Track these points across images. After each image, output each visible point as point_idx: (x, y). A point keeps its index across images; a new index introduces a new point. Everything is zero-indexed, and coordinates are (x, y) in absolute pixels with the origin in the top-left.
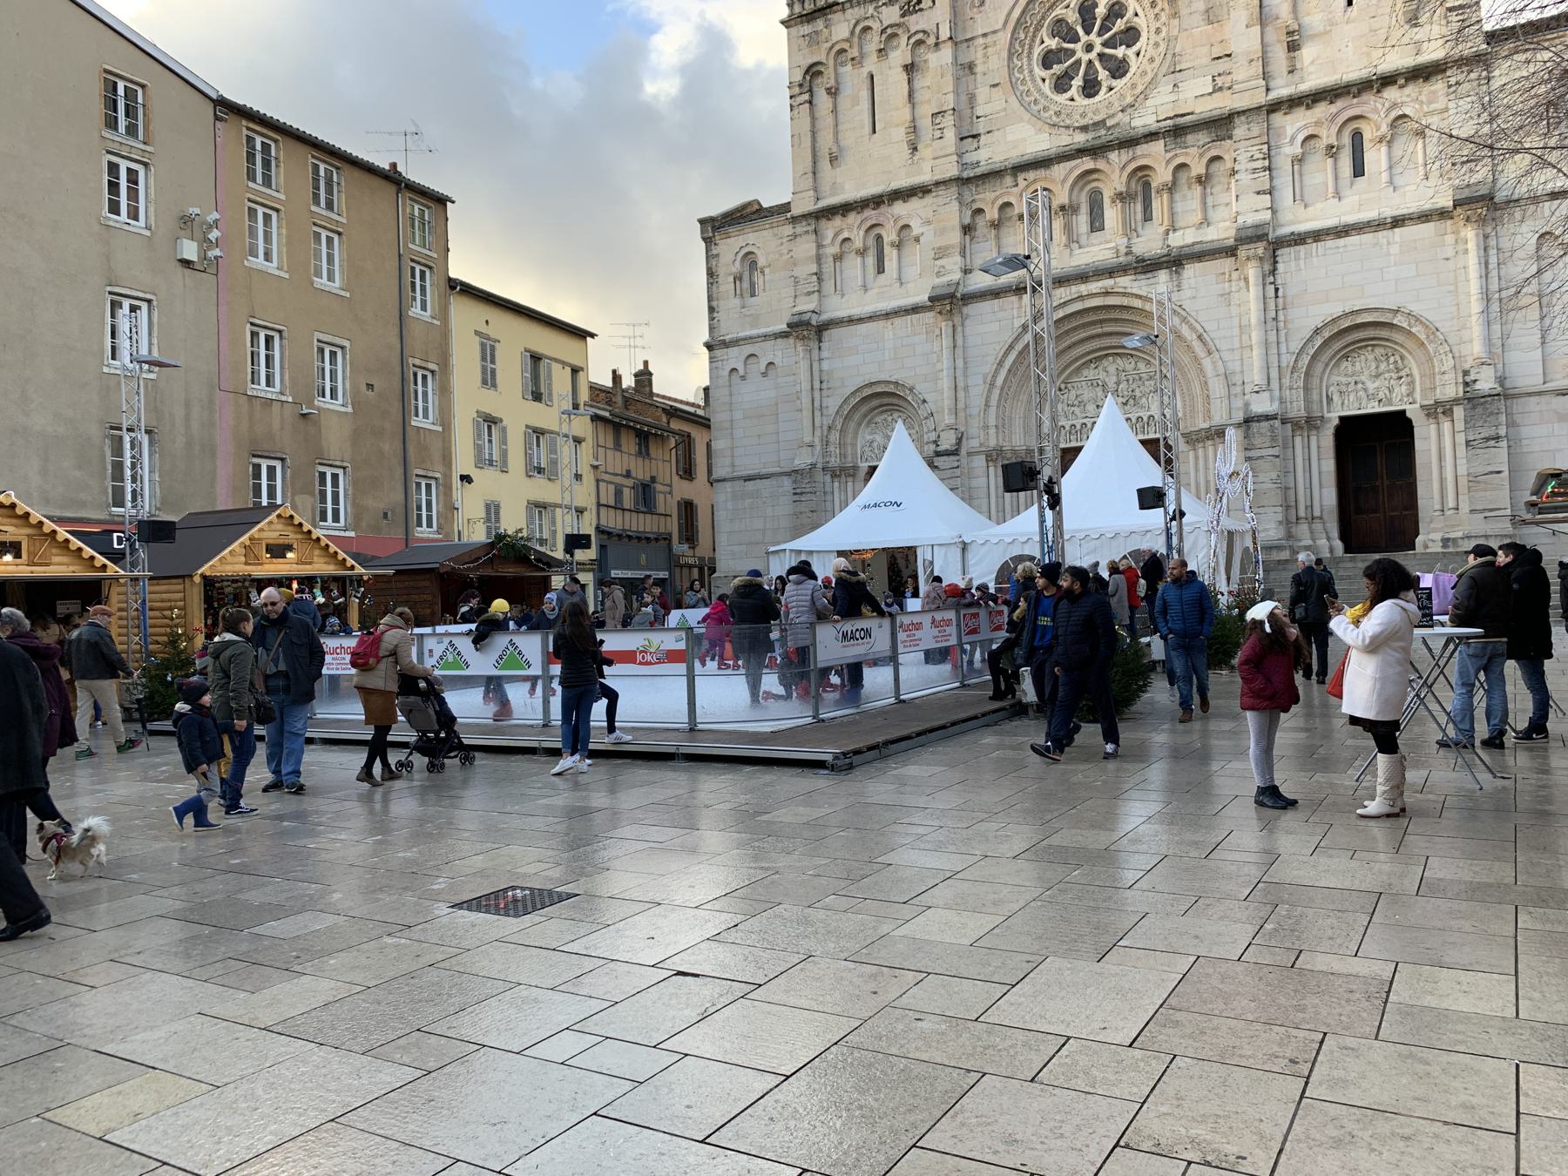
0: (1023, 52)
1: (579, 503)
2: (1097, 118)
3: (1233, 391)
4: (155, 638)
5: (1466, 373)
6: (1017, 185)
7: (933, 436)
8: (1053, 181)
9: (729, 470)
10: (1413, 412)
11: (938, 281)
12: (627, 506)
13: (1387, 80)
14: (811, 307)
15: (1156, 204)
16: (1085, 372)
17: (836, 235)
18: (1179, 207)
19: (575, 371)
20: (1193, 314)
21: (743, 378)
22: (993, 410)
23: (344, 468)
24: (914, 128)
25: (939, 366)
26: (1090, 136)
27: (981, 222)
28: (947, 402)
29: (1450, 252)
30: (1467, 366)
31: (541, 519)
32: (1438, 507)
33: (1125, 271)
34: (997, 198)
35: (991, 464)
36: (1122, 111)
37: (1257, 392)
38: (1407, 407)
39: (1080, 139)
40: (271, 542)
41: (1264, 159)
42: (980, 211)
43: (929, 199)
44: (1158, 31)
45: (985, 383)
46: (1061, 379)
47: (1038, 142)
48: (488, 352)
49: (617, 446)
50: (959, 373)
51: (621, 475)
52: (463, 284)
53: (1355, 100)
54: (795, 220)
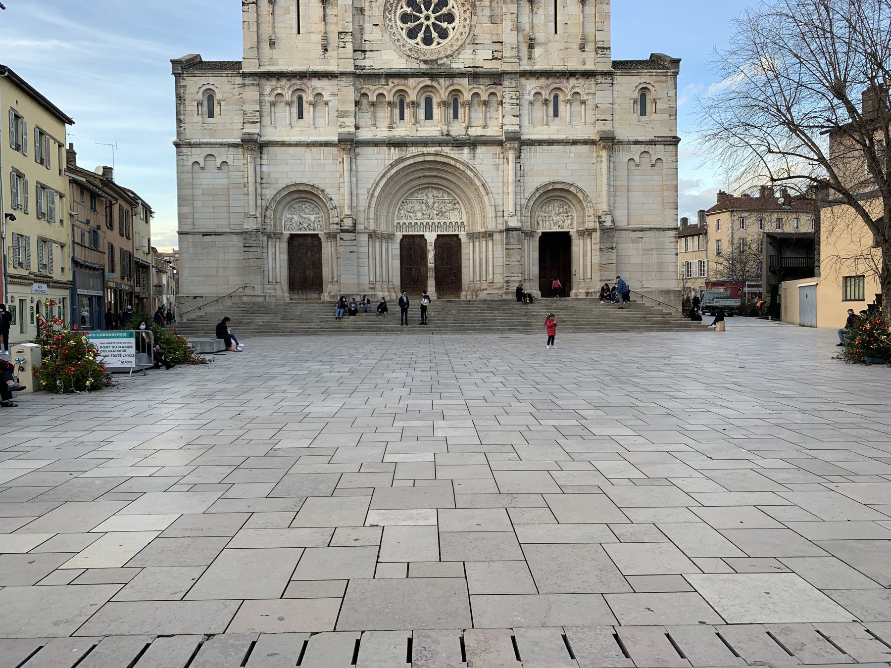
0: (392, 9)
2: (434, 58)
3: (498, 215)
5: (599, 217)
6: (388, 85)
7: (336, 220)
8: (408, 87)
9: (191, 227)
10: (573, 232)
11: (341, 130)
13: (572, 74)
14: (257, 131)
15: (460, 111)
16: (416, 195)
17: (273, 90)
18: (473, 115)
20: (481, 172)
21: (203, 169)
22: (372, 210)
24: (325, 38)
25: (341, 180)
26: (428, 67)
27: (364, 101)
28: (347, 202)
29: (594, 161)
30: (600, 214)
32: (582, 277)
33: (448, 144)
34: (376, 90)
35: (370, 240)
36: (446, 57)
37: (512, 216)
38: (570, 230)
39: (423, 66)
41: (517, 99)
42: (365, 95)
43: (334, 82)
44: (465, 19)
45: (368, 193)
46: (404, 197)
47: (399, 64)
50: (354, 186)
52: (10, 71)
53: (557, 80)
54: (245, 75)
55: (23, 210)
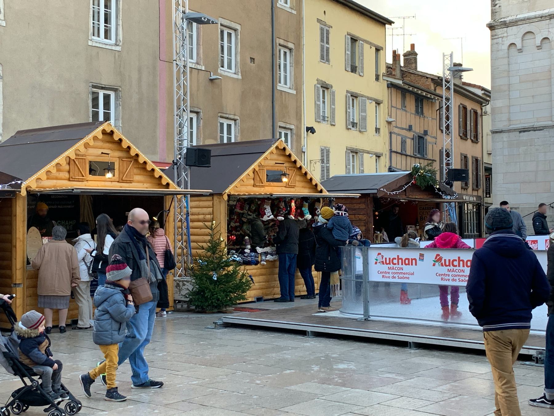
1: (378, 150)
4: (201, 244)
12: (408, 153)
19: (378, 50)
21: (520, 51)
23: (235, 120)
31: (353, 162)
40: (268, 168)
48: (325, 36)
49: (404, 106)
51: (405, 129)
55: (329, 122)
